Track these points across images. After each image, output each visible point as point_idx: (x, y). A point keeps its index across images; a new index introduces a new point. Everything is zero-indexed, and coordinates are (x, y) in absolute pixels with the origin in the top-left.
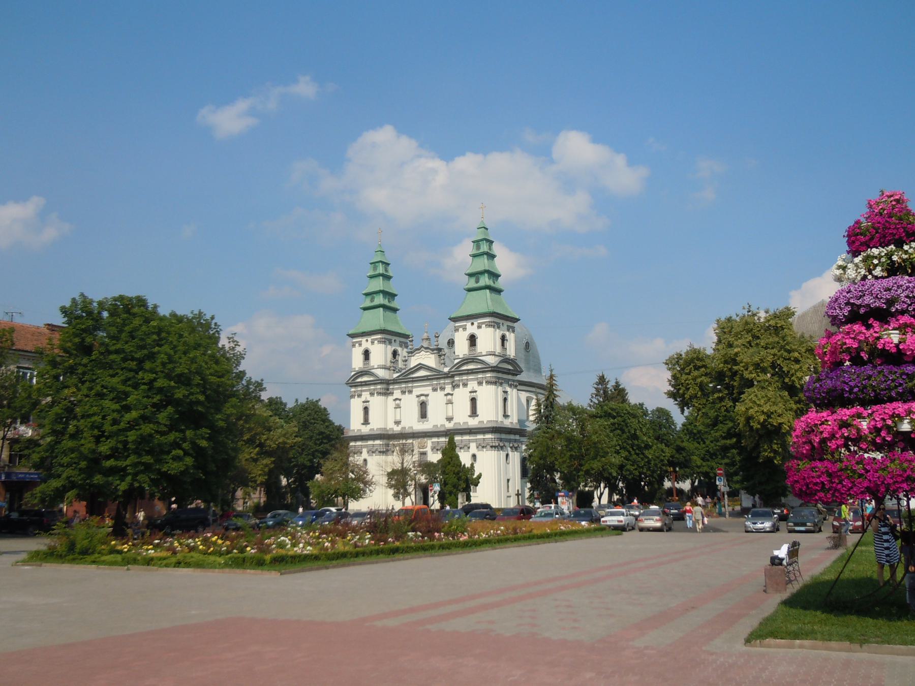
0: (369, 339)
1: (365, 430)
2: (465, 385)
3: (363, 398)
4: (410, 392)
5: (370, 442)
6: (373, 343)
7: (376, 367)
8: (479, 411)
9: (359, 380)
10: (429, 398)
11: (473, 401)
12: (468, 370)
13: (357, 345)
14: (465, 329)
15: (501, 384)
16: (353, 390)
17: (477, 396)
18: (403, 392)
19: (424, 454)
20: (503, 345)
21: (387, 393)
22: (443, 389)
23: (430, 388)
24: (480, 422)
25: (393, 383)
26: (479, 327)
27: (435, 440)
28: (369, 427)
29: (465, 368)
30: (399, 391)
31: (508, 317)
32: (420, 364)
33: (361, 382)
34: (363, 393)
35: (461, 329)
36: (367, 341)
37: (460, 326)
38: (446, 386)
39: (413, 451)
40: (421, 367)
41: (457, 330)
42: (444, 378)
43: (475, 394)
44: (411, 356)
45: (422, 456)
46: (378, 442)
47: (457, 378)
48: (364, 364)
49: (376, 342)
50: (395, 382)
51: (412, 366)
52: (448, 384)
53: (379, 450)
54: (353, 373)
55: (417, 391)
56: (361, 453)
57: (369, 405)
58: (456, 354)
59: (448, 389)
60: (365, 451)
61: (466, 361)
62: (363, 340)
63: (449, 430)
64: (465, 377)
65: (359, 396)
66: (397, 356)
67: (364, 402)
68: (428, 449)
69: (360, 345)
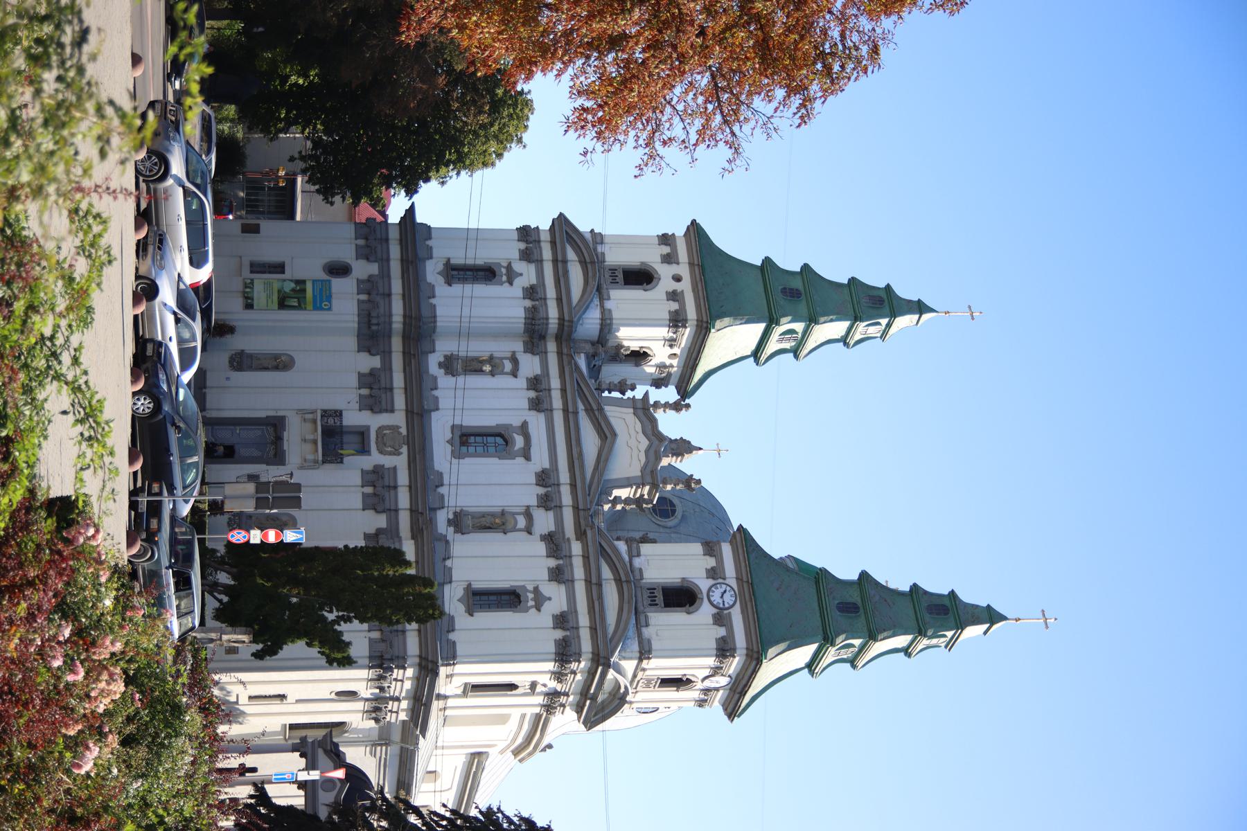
0: (686, 286)
1: (432, 272)
2: (558, 575)
3: (519, 266)
4: (537, 405)
5: (397, 286)
6: (673, 296)
7: (608, 305)
8: (487, 619)
9: (571, 255)
10: (521, 460)
11: (509, 599)
12: (600, 585)
13: (666, 250)
14: (715, 573)
15: (559, 676)
16: (545, 237)
17: (527, 610)
18: (535, 383)
19: (364, 450)
20: (667, 682)
21: (534, 335)
22: (547, 502)
23: (547, 465)
24: (452, 619)
25: (560, 354)
26: (721, 618)
27: (403, 478)
28: (441, 280)
29: (606, 573)
30: (538, 371)
31: (743, 693)
32: (614, 435)
33: (565, 262)
34: (532, 267)
35: (711, 562)
36: (677, 279)
37: (720, 561)
38: (551, 514)
39: (373, 409)
40: (606, 434)
41: (711, 549)
42: (576, 508)
43: (531, 603)
44: (635, 408)
45: (356, 439)
46: (397, 307)
47: (576, 548)
48: (613, 270)
49: (674, 306)
50: (565, 360)
51: (607, 408)
52: (559, 521)
53: (373, 314)
54: (588, 237)
55: (537, 424)
56: (368, 259)
57: (501, 284)
58: (646, 548)
59: (544, 522)
60: (373, 269)
61: (627, 579)
62: (683, 270)
63: (432, 522)
64: (579, 572)
65: (526, 256)
66: (633, 358)
67: (509, 267)
68: (375, 458)
69: (669, 259)
